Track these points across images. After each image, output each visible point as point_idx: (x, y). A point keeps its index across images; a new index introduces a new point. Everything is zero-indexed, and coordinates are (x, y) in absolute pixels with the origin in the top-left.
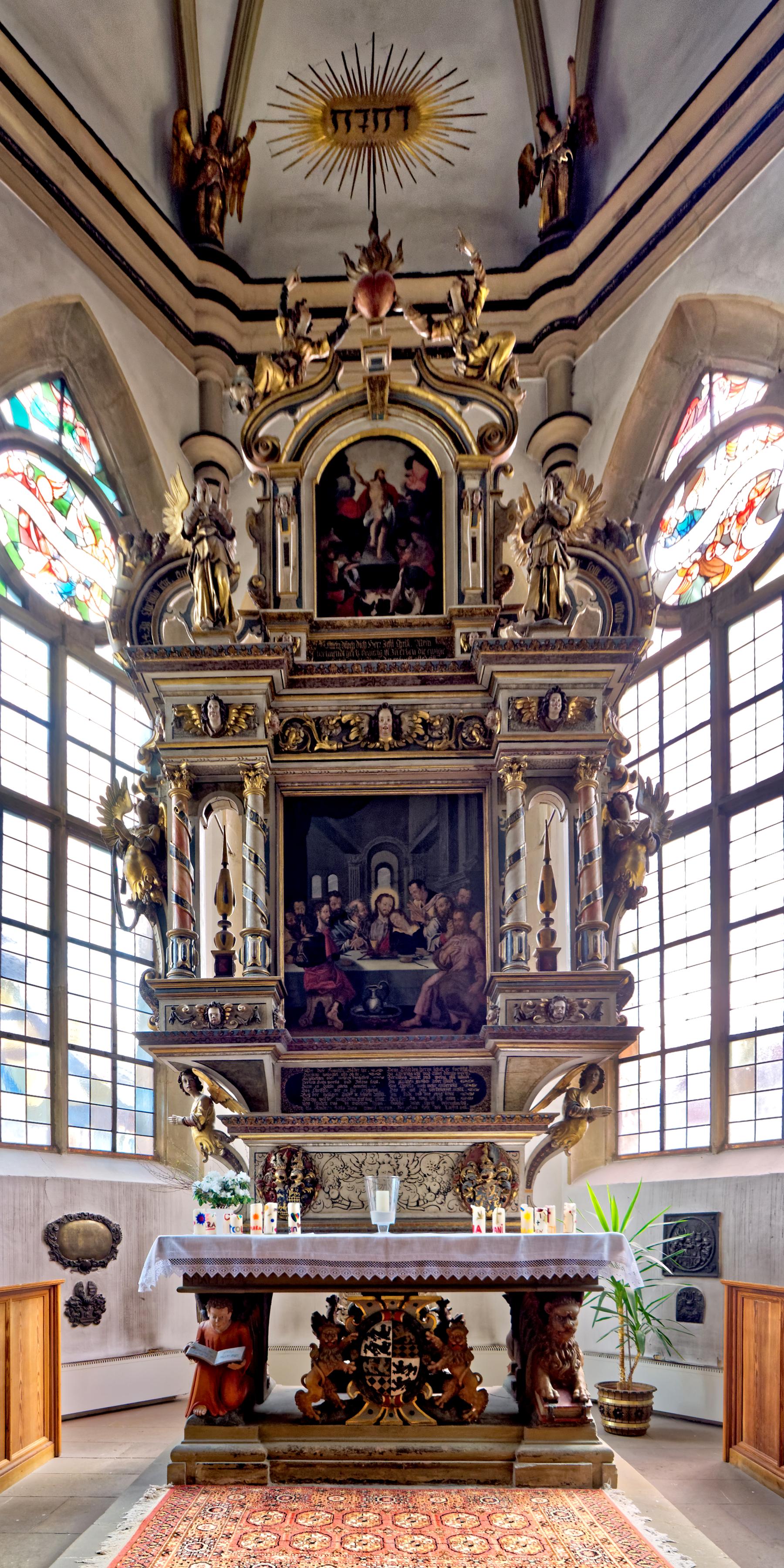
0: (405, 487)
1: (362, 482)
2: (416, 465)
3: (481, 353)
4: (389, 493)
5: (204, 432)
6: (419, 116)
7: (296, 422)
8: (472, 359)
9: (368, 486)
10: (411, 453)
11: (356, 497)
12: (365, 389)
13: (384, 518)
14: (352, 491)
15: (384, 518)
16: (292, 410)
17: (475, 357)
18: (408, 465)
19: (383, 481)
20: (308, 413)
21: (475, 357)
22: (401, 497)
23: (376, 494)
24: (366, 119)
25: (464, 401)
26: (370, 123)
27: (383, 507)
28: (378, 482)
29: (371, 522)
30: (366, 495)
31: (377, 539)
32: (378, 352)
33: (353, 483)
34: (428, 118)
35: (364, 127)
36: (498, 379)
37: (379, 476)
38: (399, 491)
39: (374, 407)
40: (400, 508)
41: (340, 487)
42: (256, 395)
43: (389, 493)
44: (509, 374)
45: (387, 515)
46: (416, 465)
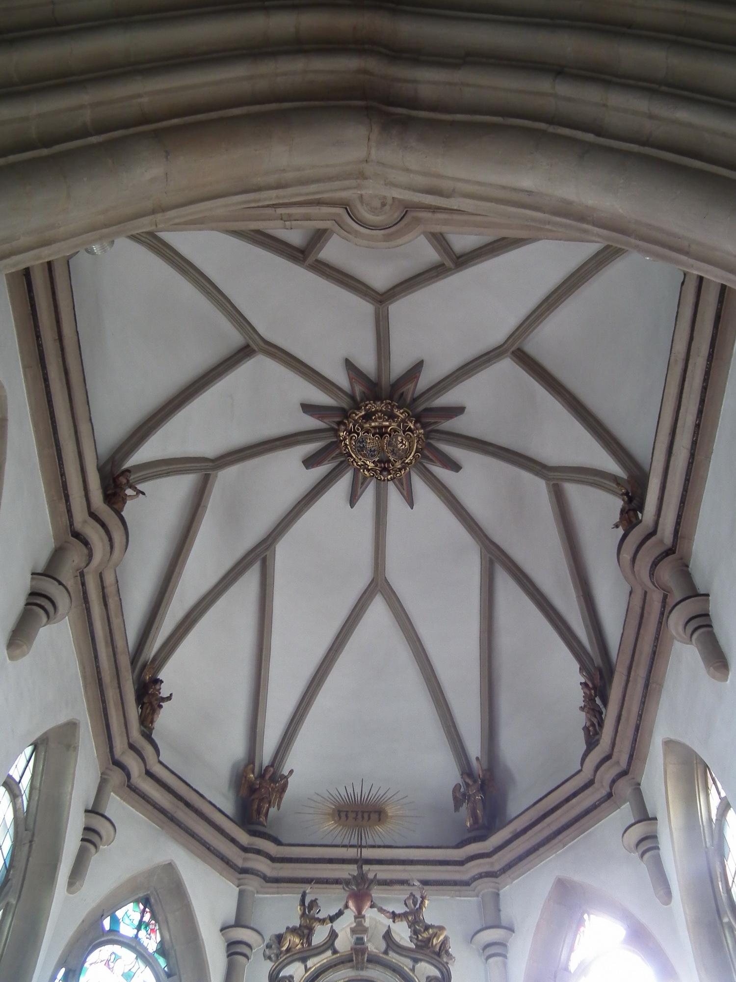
3: (425, 935)
5: (239, 923)
6: (387, 815)
7: (306, 970)
8: (420, 937)
12: (352, 954)
16: (304, 960)
17: (422, 937)
20: (314, 963)
21: (422, 937)
24: (357, 815)
25: (416, 961)
26: (360, 816)
32: (361, 934)
34: (392, 817)
35: (356, 819)
36: (437, 949)
39: (357, 963)
42: (281, 952)
44: (445, 947)
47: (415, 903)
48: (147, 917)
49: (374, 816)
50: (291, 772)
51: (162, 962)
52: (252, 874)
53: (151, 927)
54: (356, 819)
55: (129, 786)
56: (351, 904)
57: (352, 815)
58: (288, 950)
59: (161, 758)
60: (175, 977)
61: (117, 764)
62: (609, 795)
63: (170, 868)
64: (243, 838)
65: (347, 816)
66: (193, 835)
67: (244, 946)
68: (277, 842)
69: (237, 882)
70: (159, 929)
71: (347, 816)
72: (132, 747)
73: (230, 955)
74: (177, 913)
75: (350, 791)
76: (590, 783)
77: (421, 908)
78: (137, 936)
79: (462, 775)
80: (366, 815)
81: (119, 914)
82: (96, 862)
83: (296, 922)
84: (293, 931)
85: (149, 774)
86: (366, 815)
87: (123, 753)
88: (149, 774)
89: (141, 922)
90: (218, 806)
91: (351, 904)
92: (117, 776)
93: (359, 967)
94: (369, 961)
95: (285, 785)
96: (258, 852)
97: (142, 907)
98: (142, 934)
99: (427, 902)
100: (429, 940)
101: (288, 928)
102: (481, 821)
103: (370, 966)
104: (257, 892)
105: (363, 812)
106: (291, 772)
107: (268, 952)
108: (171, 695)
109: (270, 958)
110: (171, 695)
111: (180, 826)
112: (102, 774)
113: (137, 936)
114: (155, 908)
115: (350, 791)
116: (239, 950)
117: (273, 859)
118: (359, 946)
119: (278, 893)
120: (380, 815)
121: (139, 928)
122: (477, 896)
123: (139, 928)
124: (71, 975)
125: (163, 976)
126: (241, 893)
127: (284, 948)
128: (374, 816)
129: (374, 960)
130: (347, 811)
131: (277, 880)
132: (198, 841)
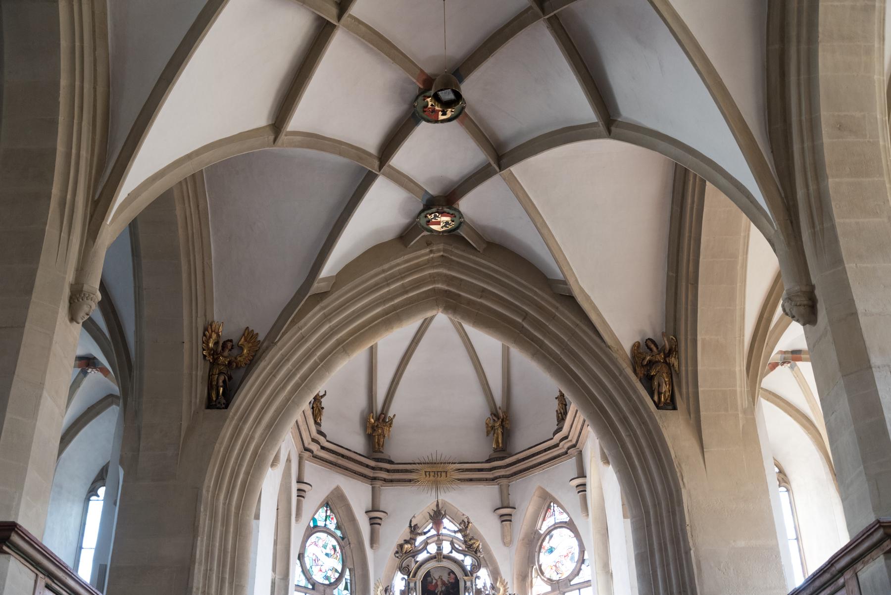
0: (448, 581)
1: (435, 579)
2: (451, 574)
4: (443, 583)
9: (437, 581)
10: (450, 571)
11: (433, 584)
13: (442, 591)
14: (432, 583)
15: (442, 591)
18: (449, 574)
19: (442, 579)
22: (447, 584)
23: (439, 583)
27: (441, 587)
28: (440, 580)
29: (438, 592)
30: (436, 583)
33: (432, 580)
37: (440, 577)
38: (446, 582)
40: (447, 587)
41: (428, 581)
43: (443, 583)
45: (443, 589)
46: (451, 574)
47: (464, 526)
48: (329, 512)
49: (444, 474)
50: (394, 416)
51: (339, 533)
52: (379, 480)
53: (331, 517)
54: (434, 476)
55: (313, 456)
56: (434, 527)
57: (432, 474)
58: (405, 553)
59: (328, 438)
60: (346, 539)
61: (306, 449)
62: (566, 453)
63: (338, 489)
64: (372, 463)
65: (430, 475)
66: (346, 469)
67: (378, 520)
68: (391, 462)
69: (370, 483)
70: (335, 516)
71: (430, 475)
72: (314, 440)
73: (371, 524)
74: (343, 508)
75: (430, 458)
76: (557, 445)
77: (467, 527)
78: (325, 525)
79: (491, 414)
80: (439, 474)
81: (316, 517)
82: (305, 502)
83: (408, 538)
84: (406, 542)
85: (323, 448)
86: (439, 474)
87: (309, 444)
88: (323, 448)
89: (326, 517)
90: (358, 452)
91: (434, 527)
92: (307, 454)
93: (439, 561)
94: (444, 558)
95: (391, 424)
96: (381, 469)
97: (325, 509)
98: (328, 522)
99: (470, 524)
100: (472, 545)
101: (405, 540)
102: (501, 445)
103: (444, 560)
104: (382, 486)
105: (438, 472)
106: (394, 416)
107: (397, 555)
108: (325, 392)
109: (397, 557)
110: (325, 392)
111: (340, 467)
112: (299, 455)
113: (325, 525)
114: (331, 507)
115: (430, 458)
116: (376, 522)
117: (388, 471)
118: (439, 551)
119: (392, 486)
120: (446, 473)
121: (326, 520)
122: (498, 484)
123: (326, 520)
124: (301, 556)
125: (340, 540)
126: (373, 488)
127: (404, 552)
128: (444, 474)
130: (430, 472)
131: (391, 481)
132: (350, 471)
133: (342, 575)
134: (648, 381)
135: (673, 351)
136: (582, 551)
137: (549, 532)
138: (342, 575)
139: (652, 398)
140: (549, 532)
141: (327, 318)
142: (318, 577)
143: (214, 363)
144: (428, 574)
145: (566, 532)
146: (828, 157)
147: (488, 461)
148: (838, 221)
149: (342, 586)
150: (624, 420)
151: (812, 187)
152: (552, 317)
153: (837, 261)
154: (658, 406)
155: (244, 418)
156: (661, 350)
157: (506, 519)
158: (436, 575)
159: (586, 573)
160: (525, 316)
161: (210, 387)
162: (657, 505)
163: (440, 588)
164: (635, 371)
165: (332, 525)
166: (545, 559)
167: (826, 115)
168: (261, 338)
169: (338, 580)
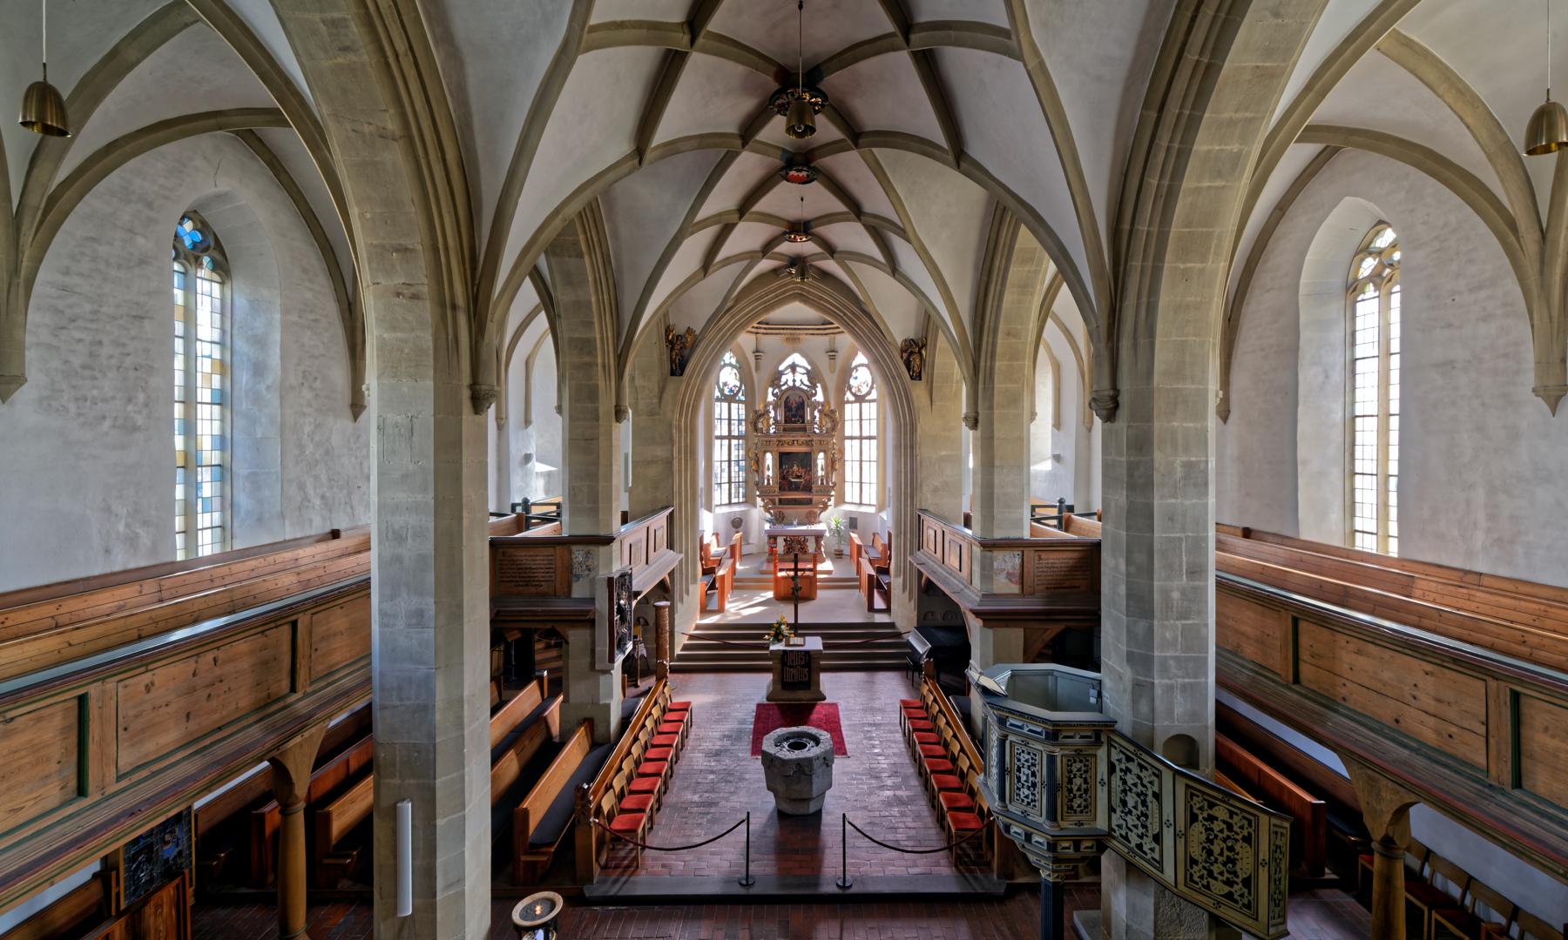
31: (794, 410)
129: (799, 388)
133: (740, 388)
134: (908, 364)
135: (924, 346)
136: (873, 383)
137: (856, 367)
138: (740, 388)
139: (909, 371)
140: (856, 367)
141: (732, 318)
142: (726, 391)
143: (672, 349)
144: (788, 398)
145: (865, 369)
146: (999, 349)
147: (823, 324)
148: (996, 386)
149: (740, 394)
150: (894, 378)
151: (988, 363)
152: (859, 319)
153: (991, 408)
154: (912, 378)
155: (691, 377)
156: (917, 345)
157: (833, 358)
158: (792, 398)
159: (874, 395)
160: (845, 314)
161: (672, 361)
162: (905, 425)
163: (794, 405)
164: (902, 357)
165: (733, 361)
166: (852, 382)
167: (1002, 327)
168: (697, 333)
169: (738, 391)
